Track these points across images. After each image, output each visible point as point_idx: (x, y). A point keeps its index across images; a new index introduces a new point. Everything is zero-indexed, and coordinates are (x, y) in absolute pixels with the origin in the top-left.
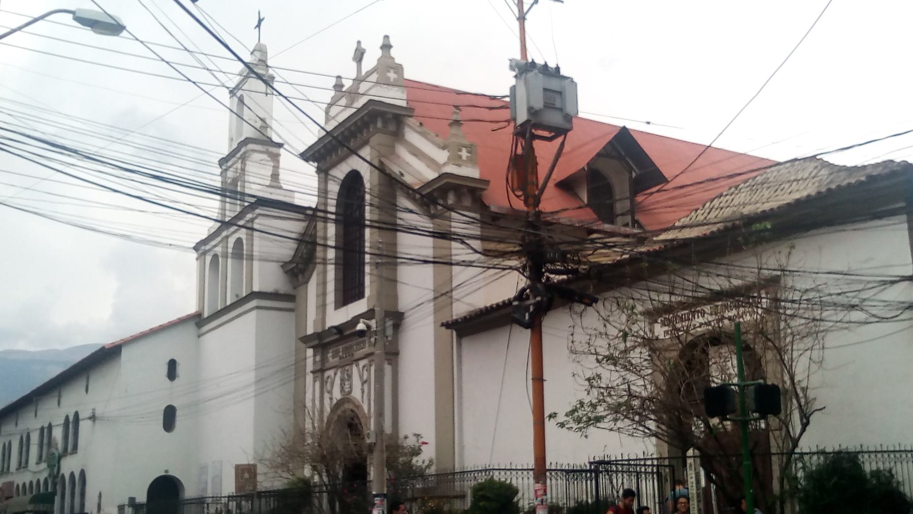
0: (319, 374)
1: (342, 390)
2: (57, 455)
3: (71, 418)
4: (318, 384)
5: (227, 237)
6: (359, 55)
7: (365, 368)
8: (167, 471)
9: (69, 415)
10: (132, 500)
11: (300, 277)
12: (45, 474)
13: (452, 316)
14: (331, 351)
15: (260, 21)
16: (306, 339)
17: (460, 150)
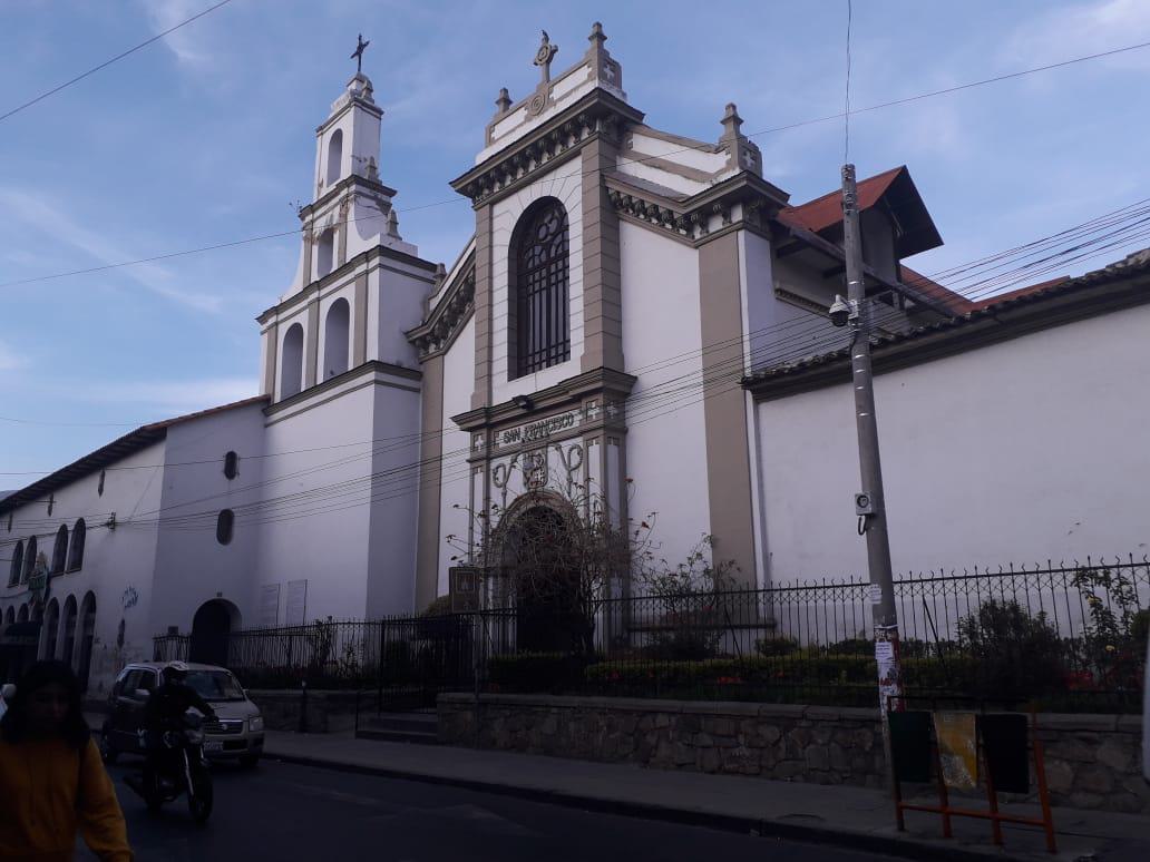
0: (484, 462)
1: (527, 481)
2: (46, 573)
3: (71, 527)
4: (480, 478)
5: (319, 299)
6: (548, 55)
7: (575, 451)
8: (220, 594)
9: (68, 524)
10: (173, 631)
11: (432, 349)
12: (25, 599)
13: (743, 369)
14: (502, 434)
15: (361, 47)
16: (458, 419)
17: (745, 154)
